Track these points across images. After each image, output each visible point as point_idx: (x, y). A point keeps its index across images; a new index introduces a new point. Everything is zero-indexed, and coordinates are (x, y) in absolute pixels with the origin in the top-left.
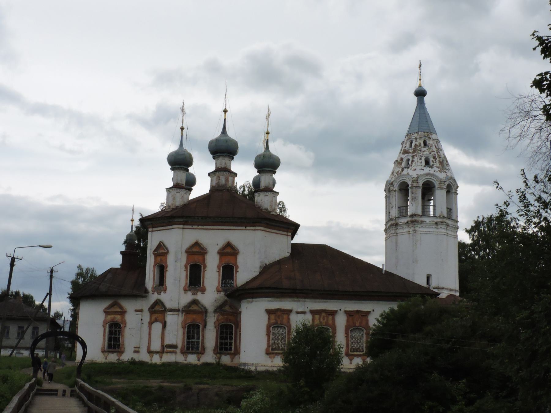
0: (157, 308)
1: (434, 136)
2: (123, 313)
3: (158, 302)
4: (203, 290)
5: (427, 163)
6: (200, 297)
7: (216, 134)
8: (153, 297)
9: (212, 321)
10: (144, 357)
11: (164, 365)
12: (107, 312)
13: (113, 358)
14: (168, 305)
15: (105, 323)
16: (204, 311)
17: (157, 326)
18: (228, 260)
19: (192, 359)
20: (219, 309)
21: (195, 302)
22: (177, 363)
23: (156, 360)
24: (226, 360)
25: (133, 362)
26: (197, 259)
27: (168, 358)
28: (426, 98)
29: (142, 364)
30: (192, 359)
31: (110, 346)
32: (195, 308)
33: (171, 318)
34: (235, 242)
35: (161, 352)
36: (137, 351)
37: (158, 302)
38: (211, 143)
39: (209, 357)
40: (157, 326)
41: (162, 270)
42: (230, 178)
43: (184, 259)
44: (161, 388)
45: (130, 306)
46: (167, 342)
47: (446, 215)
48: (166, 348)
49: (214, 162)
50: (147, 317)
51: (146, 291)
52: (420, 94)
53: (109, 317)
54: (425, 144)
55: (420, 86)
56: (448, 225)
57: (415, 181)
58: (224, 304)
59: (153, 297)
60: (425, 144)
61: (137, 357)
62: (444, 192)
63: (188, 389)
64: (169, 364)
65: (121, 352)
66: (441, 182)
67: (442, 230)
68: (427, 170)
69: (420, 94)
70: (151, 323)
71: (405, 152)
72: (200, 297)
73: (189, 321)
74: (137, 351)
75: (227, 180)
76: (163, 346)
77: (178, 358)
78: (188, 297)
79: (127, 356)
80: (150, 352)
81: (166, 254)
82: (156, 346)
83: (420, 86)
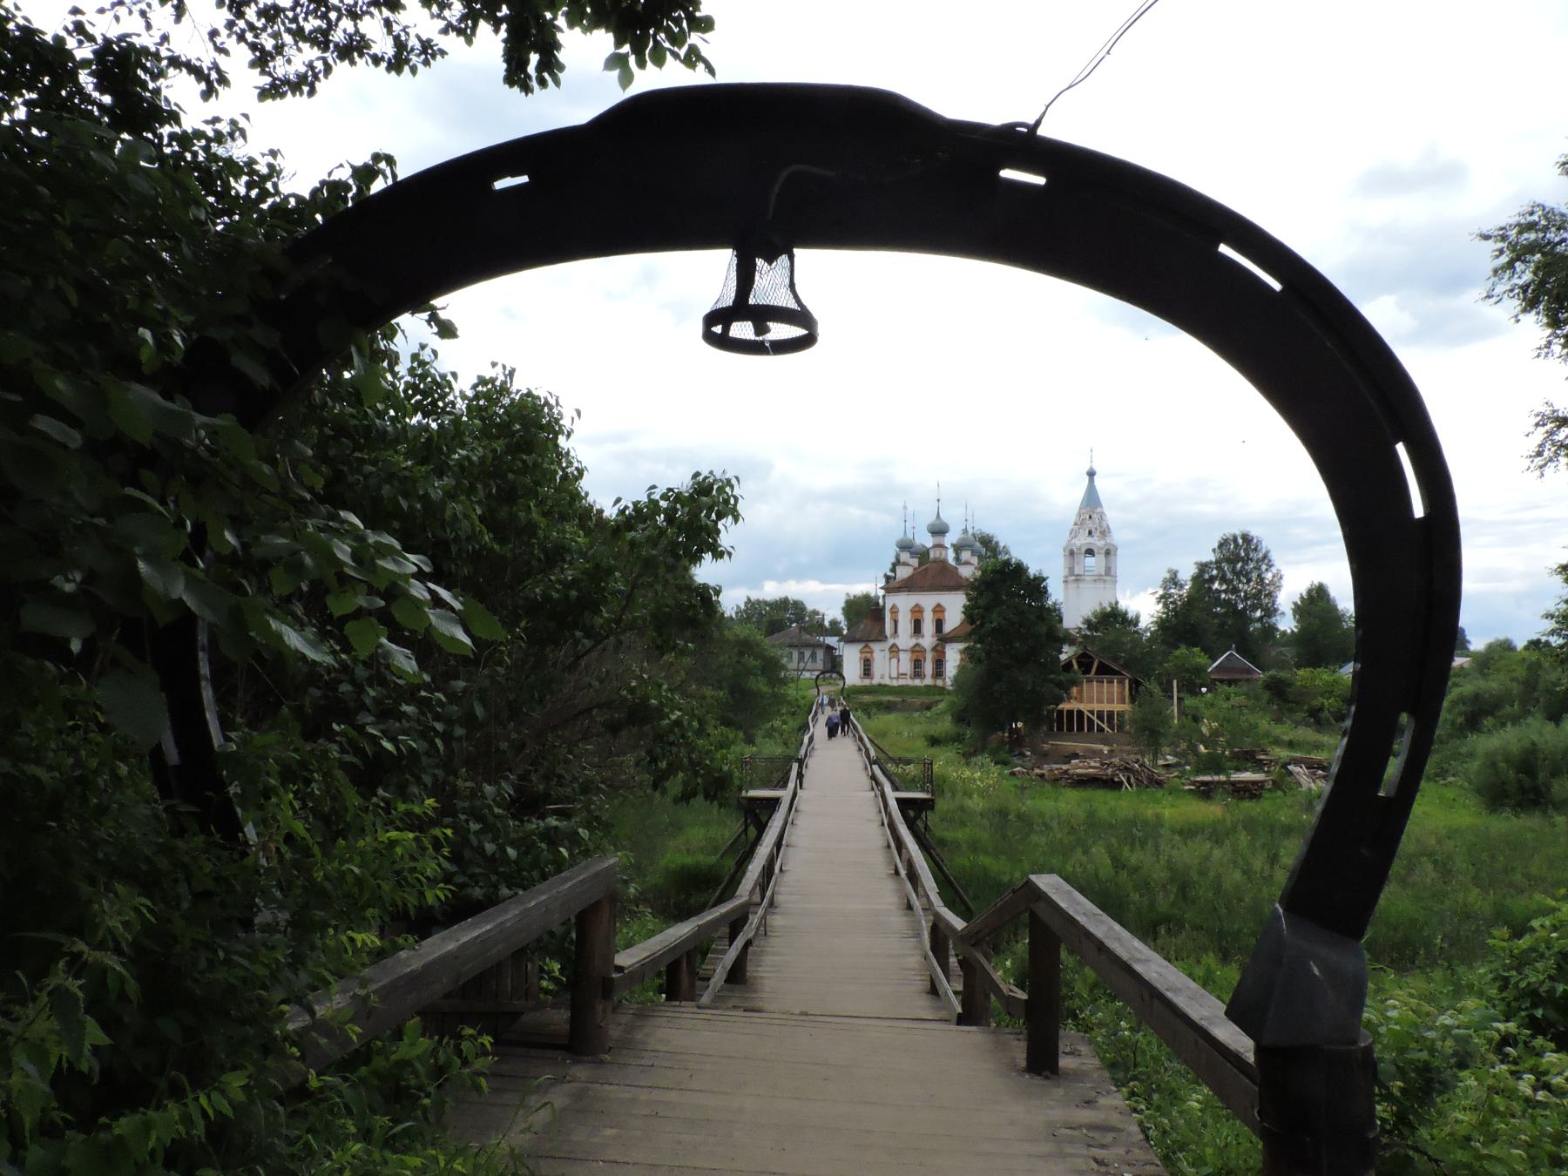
0: (894, 649)
1: (1098, 510)
2: (872, 652)
3: (894, 645)
4: (923, 636)
5: (1090, 533)
6: (920, 641)
7: (932, 519)
8: (891, 641)
9: (929, 657)
10: (887, 681)
11: (899, 686)
12: (861, 652)
13: (867, 682)
14: (901, 648)
15: (861, 659)
16: (924, 651)
17: (894, 661)
18: (939, 616)
19: (917, 682)
20: (934, 649)
21: (917, 645)
22: (907, 685)
23: (895, 683)
24: (939, 683)
25: (880, 685)
26: (918, 616)
27: (902, 682)
28: (1095, 477)
29: (885, 686)
30: (917, 682)
31: (865, 674)
32: (917, 648)
33: (902, 656)
34: (943, 604)
35: (898, 678)
36: (882, 677)
37: (894, 645)
38: (929, 526)
39: (928, 681)
40: (894, 661)
41: (896, 623)
42: (944, 552)
43: (909, 615)
44: (889, 701)
45: (876, 647)
46: (901, 672)
47: (1103, 573)
48: (901, 675)
49: (931, 538)
50: (887, 654)
51: (886, 637)
52: (1091, 474)
53: (864, 655)
54: (1090, 517)
55: (1091, 468)
56: (1105, 581)
57: (1080, 549)
58: (937, 645)
59: (891, 641)
60: (1090, 517)
61: (883, 682)
62: (1103, 557)
63: (903, 701)
64: (903, 686)
65: (872, 678)
66: (1099, 548)
67: (1100, 585)
68: (1090, 540)
69: (1091, 474)
70: (890, 659)
71: (1076, 524)
72: (920, 641)
73: (915, 657)
74: (882, 677)
75: (941, 554)
76: (899, 674)
77: (908, 682)
78: (913, 642)
79: (875, 681)
80: (890, 678)
81: (897, 612)
82: (894, 674)
83: (1091, 468)
